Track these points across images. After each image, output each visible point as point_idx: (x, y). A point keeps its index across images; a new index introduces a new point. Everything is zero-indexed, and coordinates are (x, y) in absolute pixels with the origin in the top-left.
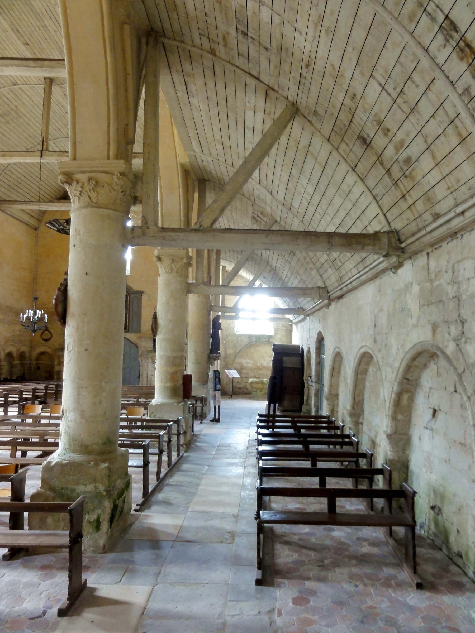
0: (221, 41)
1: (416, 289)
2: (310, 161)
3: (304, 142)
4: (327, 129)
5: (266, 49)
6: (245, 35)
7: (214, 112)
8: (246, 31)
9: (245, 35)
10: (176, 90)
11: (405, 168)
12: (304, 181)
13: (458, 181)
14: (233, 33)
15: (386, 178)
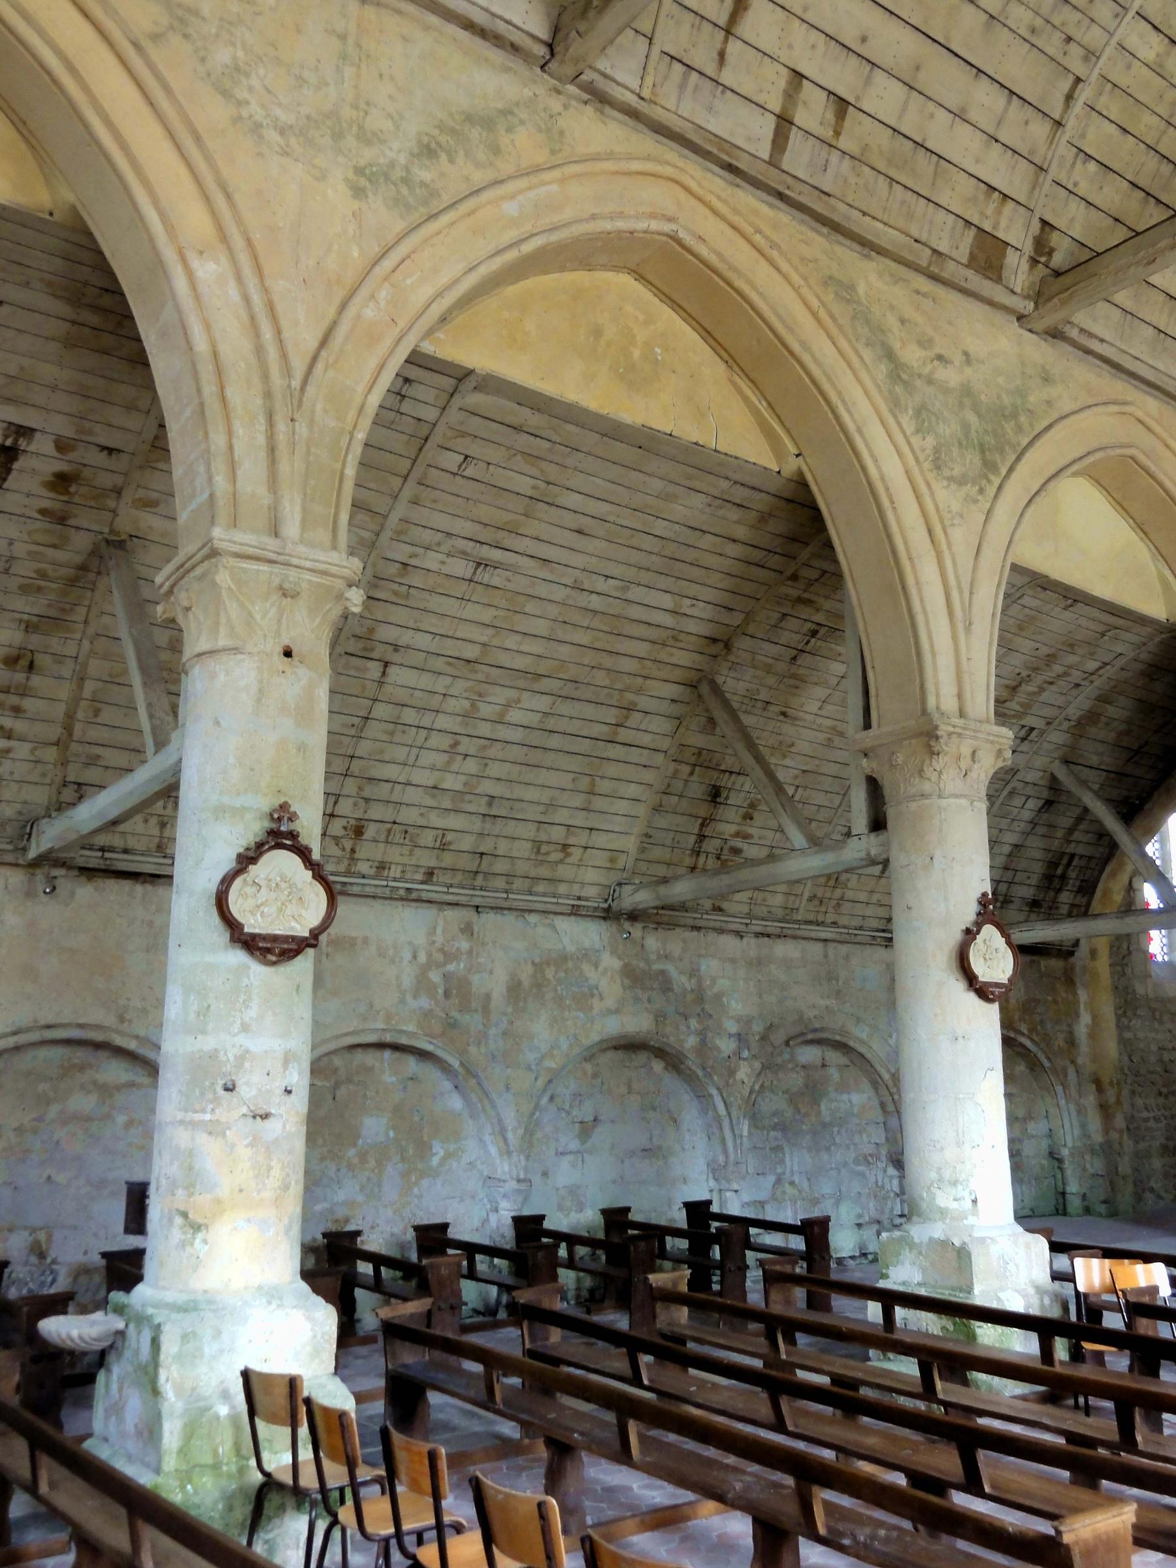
0: (806, 595)
1: (610, 962)
2: (611, 716)
3: (643, 702)
4: (698, 740)
5: (794, 658)
6: (814, 633)
7: (659, 527)
8: (818, 636)
9: (814, 633)
10: (735, 483)
11: (725, 852)
12: (543, 703)
13: (764, 900)
14: (819, 618)
15: (693, 839)
